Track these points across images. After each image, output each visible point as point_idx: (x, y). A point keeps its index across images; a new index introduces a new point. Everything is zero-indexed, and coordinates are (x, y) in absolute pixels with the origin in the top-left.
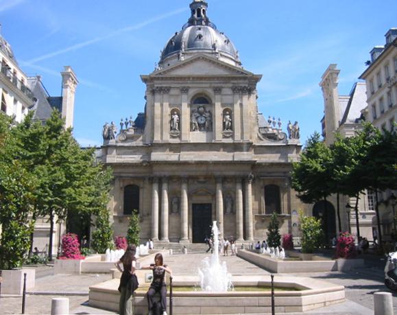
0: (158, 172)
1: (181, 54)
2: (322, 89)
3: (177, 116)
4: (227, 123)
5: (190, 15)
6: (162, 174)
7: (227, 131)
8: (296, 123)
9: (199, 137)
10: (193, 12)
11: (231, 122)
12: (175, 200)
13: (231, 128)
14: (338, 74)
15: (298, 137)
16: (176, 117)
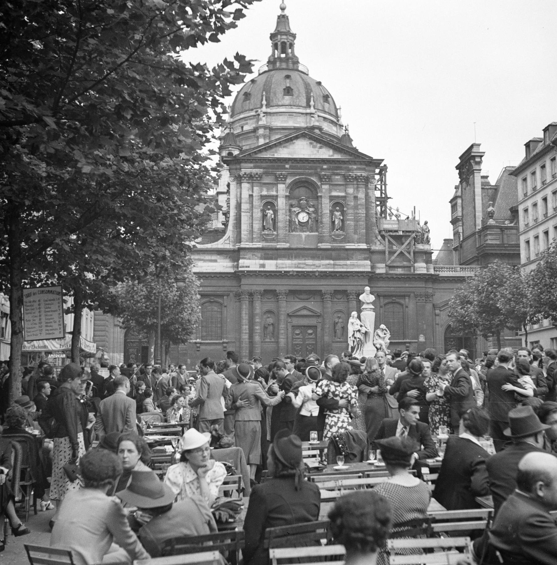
0: (247, 285)
1: (262, 115)
2: (460, 174)
3: (271, 212)
4: (336, 223)
5: (270, 53)
6: (254, 288)
7: (337, 232)
8: (426, 223)
9: (303, 238)
10: (275, 46)
11: (343, 221)
12: (270, 321)
13: (342, 228)
14: (481, 156)
15: (428, 241)
16: (270, 212)
